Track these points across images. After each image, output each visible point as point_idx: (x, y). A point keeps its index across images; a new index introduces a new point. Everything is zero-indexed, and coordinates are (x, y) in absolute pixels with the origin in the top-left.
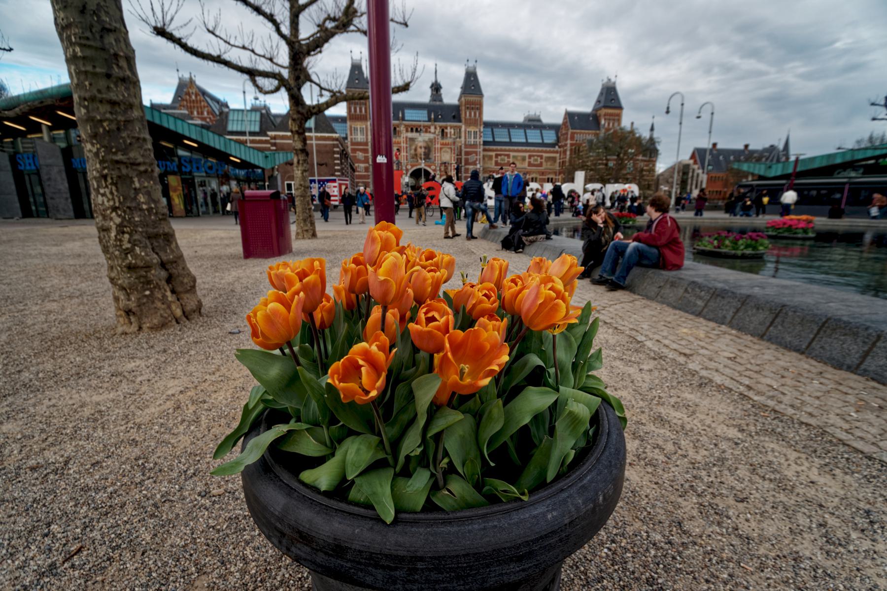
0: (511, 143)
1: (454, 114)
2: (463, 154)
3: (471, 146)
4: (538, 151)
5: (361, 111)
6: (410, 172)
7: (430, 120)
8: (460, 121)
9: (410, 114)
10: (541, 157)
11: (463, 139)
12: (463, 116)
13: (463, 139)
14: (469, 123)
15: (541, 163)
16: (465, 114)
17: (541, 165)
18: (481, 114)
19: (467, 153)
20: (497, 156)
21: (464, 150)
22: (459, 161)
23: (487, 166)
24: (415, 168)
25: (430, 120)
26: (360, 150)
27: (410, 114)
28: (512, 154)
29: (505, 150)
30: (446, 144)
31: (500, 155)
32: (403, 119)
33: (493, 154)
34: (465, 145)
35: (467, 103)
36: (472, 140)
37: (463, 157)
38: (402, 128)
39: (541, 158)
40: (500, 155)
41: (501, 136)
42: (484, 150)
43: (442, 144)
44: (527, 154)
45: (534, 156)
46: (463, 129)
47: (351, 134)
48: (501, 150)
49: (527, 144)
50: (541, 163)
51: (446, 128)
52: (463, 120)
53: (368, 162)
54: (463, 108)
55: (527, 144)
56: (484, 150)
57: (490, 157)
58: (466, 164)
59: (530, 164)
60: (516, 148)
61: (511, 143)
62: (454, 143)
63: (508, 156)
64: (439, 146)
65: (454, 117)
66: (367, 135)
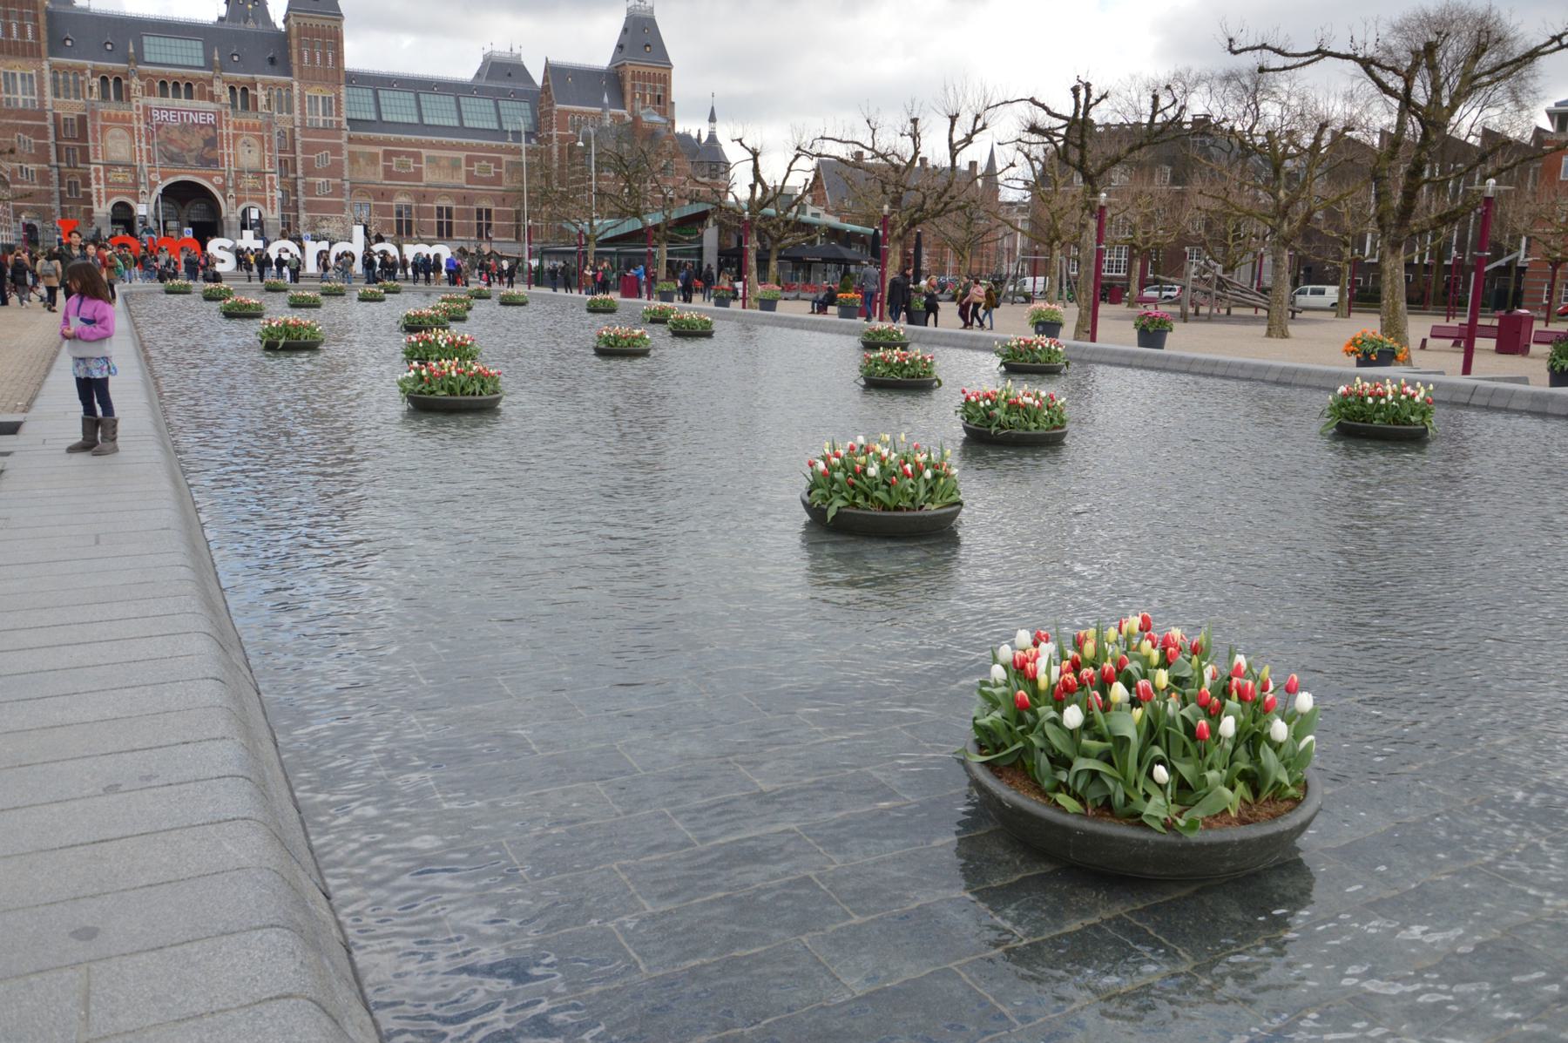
0: (421, 127)
1: (276, 52)
2: (298, 149)
4: (492, 150)
6: (159, 190)
7: (209, 65)
8: (289, 73)
9: (155, 49)
10: (498, 163)
11: (297, 111)
12: (295, 60)
13: (297, 111)
14: (309, 78)
15: (499, 175)
16: (300, 55)
17: (498, 179)
18: (339, 56)
19: (308, 148)
20: (388, 155)
22: (286, 166)
23: (362, 177)
24: (171, 180)
25: (209, 65)
26: (26, 129)
27: (155, 49)
28: (425, 152)
29: (411, 144)
31: (398, 154)
32: (139, 58)
33: (379, 150)
34: (303, 127)
35: (304, 31)
36: (321, 118)
37: (300, 156)
38: (135, 83)
39: (499, 165)
40: (398, 154)
41: (398, 108)
42: (350, 140)
43: (238, 127)
44: (462, 155)
45: (479, 159)
46: (296, 91)
48: (399, 143)
49: (461, 130)
50: (499, 175)
52: (296, 70)
53: (47, 161)
54: (294, 42)
55: (461, 130)
56: (350, 140)
57: (373, 158)
58: (306, 174)
59: (470, 178)
60: (434, 139)
61: (421, 127)
63: (417, 157)
64: (231, 131)
65: (272, 61)
66: (41, 93)
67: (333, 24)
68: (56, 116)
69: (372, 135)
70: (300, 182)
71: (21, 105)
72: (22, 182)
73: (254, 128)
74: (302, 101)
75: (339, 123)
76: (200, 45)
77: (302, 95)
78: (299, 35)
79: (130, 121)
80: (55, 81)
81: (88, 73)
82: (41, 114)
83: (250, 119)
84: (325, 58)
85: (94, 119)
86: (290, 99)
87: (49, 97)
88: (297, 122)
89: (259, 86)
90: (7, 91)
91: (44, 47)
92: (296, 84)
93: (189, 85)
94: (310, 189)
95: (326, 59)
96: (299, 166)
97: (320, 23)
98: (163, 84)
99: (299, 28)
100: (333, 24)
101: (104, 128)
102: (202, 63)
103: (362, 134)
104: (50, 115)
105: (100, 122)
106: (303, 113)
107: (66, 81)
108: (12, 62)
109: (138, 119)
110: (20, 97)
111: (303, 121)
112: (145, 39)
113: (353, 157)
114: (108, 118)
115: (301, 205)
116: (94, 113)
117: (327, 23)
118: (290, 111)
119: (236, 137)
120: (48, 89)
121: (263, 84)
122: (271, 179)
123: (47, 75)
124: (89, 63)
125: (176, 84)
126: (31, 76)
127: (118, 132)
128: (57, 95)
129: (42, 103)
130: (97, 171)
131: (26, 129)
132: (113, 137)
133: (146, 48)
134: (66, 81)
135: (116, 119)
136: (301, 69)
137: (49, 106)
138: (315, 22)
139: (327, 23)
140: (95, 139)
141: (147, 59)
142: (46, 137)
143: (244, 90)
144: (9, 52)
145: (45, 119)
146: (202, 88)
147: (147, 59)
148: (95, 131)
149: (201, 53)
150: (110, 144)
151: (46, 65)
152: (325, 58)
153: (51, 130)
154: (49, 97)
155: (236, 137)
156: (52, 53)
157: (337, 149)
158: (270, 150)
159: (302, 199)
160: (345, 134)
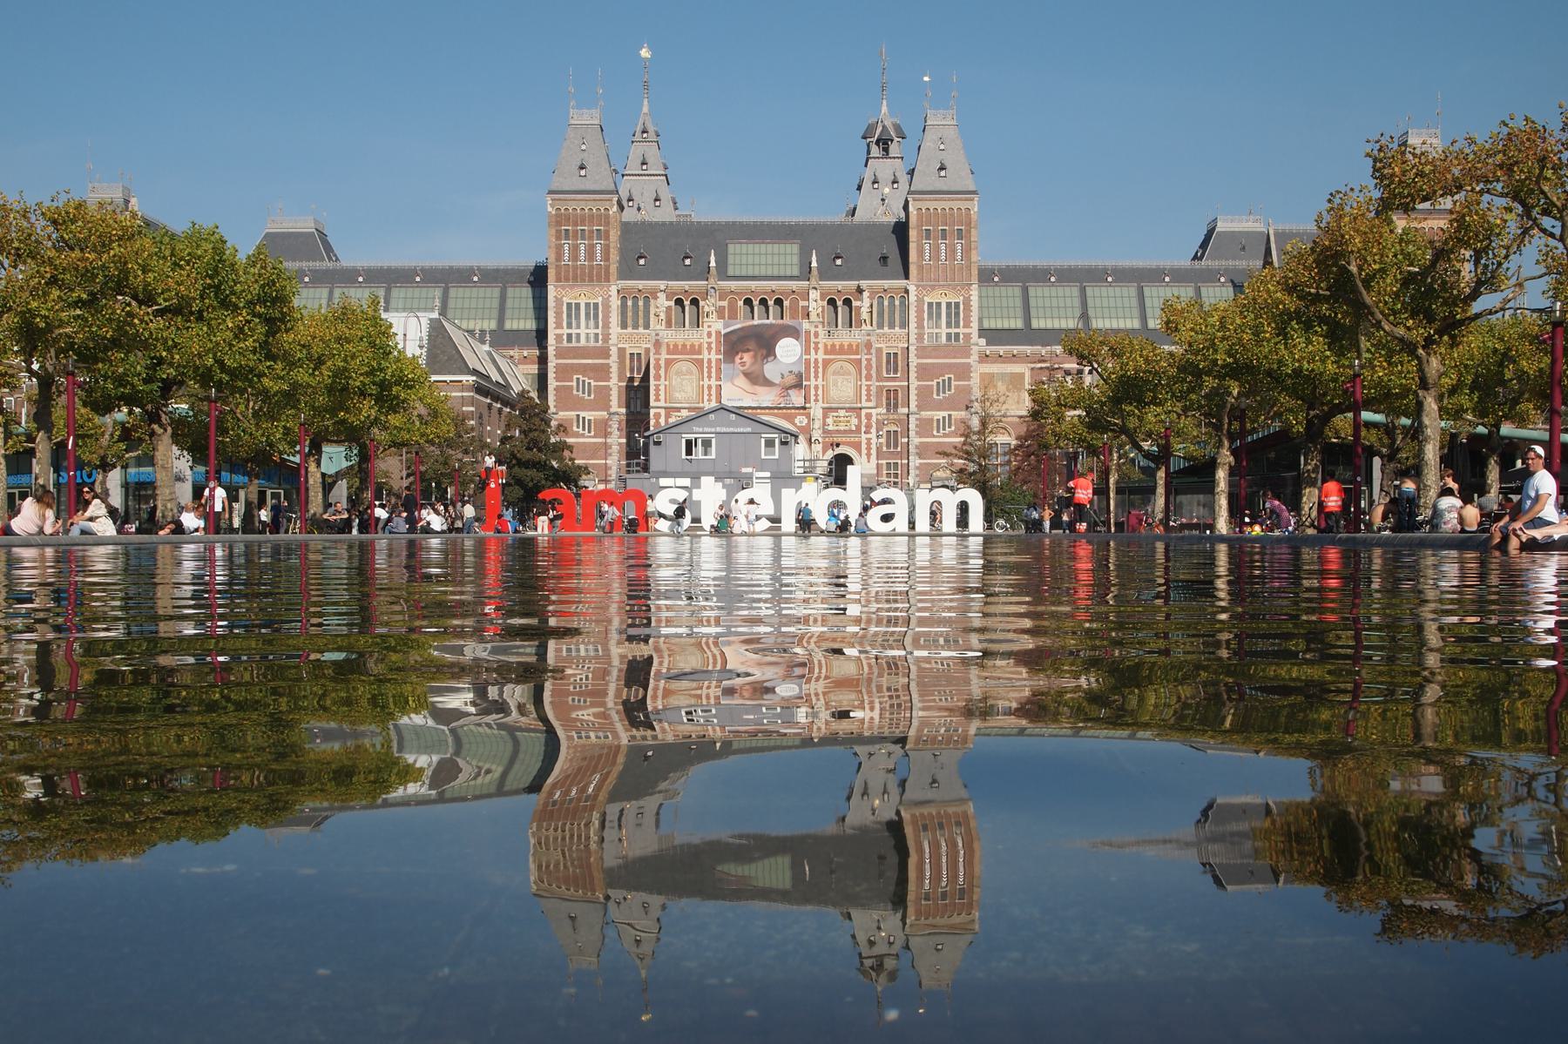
2: (913, 375)
3: (936, 350)
5: (591, 254)
7: (806, 273)
8: (907, 277)
13: (913, 325)
19: (924, 372)
21: (914, 361)
22: (892, 400)
25: (806, 273)
26: (584, 370)
30: (842, 351)
36: (944, 330)
37: (914, 383)
38: (706, 306)
43: (831, 350)
46: (912, 298)
47: (559, 325)
51: (860, 291)
53: (607, 407)
58: (920, 407)
62: (869, 345)
64: (821, 356)
66: (606, 325)
67: (963, 205)
68: (621, 351)
69: (1016, 349)
70: (912, 419)
71: (583, 342)
72: (577, 435)
73: (852, 350)
74: (920, 311)
75: (968, 336)
76: (795, 248)
77: (920, 301)
78: (920, 225)
79: (700, 353)
80: (624, 306)
81: (662, 296)
82: (604, 353)
83: (845, 337)
84: (952, 251)
85: (657, 352)
86: (905, 306)
87: (615, 329)
88: (913, 339)
89: (866, 294)
90: (569, 326)
91: (613, 268)
92: (912, 289)
93: (779, 302)
94: (925, 427)
95: (954, 251)
96: (913, 397)
97: (947, 205)
98: (748, 302)
99: (920, 216)
100: (963, 205)
101: (669, 363)
102: (796, 272)
103: (1001, 350)
104: (614, 351)
105: (664, 356)
106: (920, 326)
107: (635, 305)
108: (577, 291)
109: (709, 349)
110: (583, 331)
111: (920, 337)
112: (731, 248)
113: (987, 381)
114: (674, 350)
115: (912, 449)
116: (657, 344)
117: (955, 205)
118: (904, 324)
119: (826, 363)
120: (615, 318)
121: (871, 291)
122: (869, 416)
123: (615, 303)
124: (662, 284)
125: (763, 302)
126: (596, 305)
127: (684, 366)
128: (624, 326)
129: (606, 338)
130: (658, 416)
131: (584, 370)
132: (678, 373)
133: (731, 260)
134: (635, 305)
135: (683, 350)
136: (920, 268)
137: (613, 339)
138: (939, 205)
139: (955, 205)
140: (658, 377)
141: (730, 272)
142: (608, 379)
143: (847, 302)
144: (575, 279)
145: (608, 356)
146: (795, 302)
147: (730, 272)
148: (658, 367)
149: (796, 259)
150: (675, 381)
151: (614, 289)
152: (952, 251)
153: (614, 369)
154: (615, 329)
155: (826, 363)
156: (623, 275)
157: (964, 372)
158: (869, 378)
159: (916, 440)
160: (975, 349)
